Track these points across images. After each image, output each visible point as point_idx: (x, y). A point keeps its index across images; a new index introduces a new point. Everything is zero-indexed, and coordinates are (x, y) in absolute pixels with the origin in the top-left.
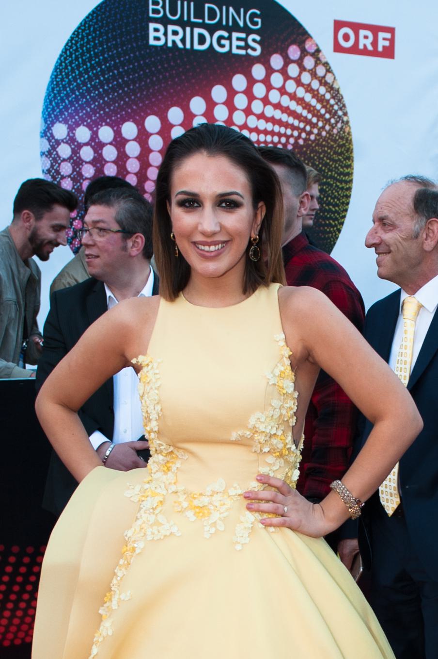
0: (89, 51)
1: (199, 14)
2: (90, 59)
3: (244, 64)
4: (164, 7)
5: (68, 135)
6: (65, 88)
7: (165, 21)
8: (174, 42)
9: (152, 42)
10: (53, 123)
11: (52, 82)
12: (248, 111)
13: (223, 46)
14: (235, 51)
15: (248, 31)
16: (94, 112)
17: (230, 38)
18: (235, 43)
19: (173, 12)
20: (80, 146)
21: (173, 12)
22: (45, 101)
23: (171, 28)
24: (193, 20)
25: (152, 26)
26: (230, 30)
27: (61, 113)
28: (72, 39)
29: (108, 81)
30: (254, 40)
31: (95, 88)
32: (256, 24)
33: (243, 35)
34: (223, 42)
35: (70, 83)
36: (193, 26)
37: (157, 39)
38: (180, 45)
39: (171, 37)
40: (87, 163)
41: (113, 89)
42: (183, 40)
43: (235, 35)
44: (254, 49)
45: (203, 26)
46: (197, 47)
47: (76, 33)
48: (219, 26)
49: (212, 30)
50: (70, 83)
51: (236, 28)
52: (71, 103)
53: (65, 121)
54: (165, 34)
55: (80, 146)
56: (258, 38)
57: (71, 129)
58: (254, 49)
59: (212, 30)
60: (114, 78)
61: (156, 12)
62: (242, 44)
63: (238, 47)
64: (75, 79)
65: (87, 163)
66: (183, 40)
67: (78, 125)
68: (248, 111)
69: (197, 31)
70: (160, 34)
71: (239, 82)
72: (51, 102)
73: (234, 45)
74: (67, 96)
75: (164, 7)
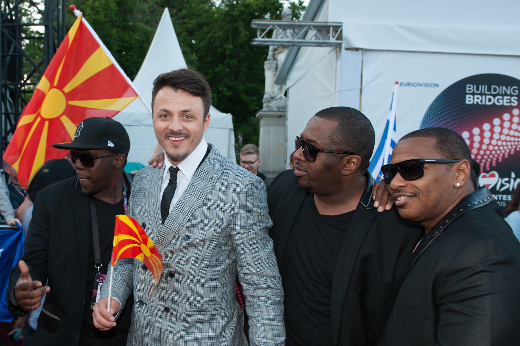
0: (439, 107)
1: (489, 90)
2: (440, 110)
3: (509, 109)
4: (473, 88)
6: (428, 122)
7: (473, 94)
8: (477, 102)
9: (467, 102)
11: (423, 120)
12: (510, 129)
13: (499, 102)
14: (505, 104)
15: (511, 95)
17: (503, 99)
18: (505, 101)
19: (477, 90)
21: (477, 90)
23: (476, 96)
24: (486, 92)
25: (467, 96)
26: (503, 95)
28: (433, 103)
29: (447, 119)
30: (514, 99)
31: (441, 121)
32: (515, 92)
33: (509, 97)
34: (500, 101)
35: (431, 120)
36: (486, 95)
37: (470, 101)
38: (480, 103)
39: (476, 100)
41: (449, 122)
42: (481, 101)
43: (505, 98)
44: (514, 103)
45: (491, 95)
46: (488, 103)
47: (435, 101)
48: (498, 94)
49: (494, 96)
50: (431, 120)
51: (506, 94)
54: (473, 99)
56: (516, 98)
58: (514, 103)
59: (494, 96)
60: (450, 117)
61: (469, 90)
62: (508, 101)
63: (507, 103)
64: (433, 118)
66: (481, 101)
68: (510, 129)
69: (488, 97)
70: (471, 99)
71: (506, 116)
73: (505, 102)
75: (473, 88)
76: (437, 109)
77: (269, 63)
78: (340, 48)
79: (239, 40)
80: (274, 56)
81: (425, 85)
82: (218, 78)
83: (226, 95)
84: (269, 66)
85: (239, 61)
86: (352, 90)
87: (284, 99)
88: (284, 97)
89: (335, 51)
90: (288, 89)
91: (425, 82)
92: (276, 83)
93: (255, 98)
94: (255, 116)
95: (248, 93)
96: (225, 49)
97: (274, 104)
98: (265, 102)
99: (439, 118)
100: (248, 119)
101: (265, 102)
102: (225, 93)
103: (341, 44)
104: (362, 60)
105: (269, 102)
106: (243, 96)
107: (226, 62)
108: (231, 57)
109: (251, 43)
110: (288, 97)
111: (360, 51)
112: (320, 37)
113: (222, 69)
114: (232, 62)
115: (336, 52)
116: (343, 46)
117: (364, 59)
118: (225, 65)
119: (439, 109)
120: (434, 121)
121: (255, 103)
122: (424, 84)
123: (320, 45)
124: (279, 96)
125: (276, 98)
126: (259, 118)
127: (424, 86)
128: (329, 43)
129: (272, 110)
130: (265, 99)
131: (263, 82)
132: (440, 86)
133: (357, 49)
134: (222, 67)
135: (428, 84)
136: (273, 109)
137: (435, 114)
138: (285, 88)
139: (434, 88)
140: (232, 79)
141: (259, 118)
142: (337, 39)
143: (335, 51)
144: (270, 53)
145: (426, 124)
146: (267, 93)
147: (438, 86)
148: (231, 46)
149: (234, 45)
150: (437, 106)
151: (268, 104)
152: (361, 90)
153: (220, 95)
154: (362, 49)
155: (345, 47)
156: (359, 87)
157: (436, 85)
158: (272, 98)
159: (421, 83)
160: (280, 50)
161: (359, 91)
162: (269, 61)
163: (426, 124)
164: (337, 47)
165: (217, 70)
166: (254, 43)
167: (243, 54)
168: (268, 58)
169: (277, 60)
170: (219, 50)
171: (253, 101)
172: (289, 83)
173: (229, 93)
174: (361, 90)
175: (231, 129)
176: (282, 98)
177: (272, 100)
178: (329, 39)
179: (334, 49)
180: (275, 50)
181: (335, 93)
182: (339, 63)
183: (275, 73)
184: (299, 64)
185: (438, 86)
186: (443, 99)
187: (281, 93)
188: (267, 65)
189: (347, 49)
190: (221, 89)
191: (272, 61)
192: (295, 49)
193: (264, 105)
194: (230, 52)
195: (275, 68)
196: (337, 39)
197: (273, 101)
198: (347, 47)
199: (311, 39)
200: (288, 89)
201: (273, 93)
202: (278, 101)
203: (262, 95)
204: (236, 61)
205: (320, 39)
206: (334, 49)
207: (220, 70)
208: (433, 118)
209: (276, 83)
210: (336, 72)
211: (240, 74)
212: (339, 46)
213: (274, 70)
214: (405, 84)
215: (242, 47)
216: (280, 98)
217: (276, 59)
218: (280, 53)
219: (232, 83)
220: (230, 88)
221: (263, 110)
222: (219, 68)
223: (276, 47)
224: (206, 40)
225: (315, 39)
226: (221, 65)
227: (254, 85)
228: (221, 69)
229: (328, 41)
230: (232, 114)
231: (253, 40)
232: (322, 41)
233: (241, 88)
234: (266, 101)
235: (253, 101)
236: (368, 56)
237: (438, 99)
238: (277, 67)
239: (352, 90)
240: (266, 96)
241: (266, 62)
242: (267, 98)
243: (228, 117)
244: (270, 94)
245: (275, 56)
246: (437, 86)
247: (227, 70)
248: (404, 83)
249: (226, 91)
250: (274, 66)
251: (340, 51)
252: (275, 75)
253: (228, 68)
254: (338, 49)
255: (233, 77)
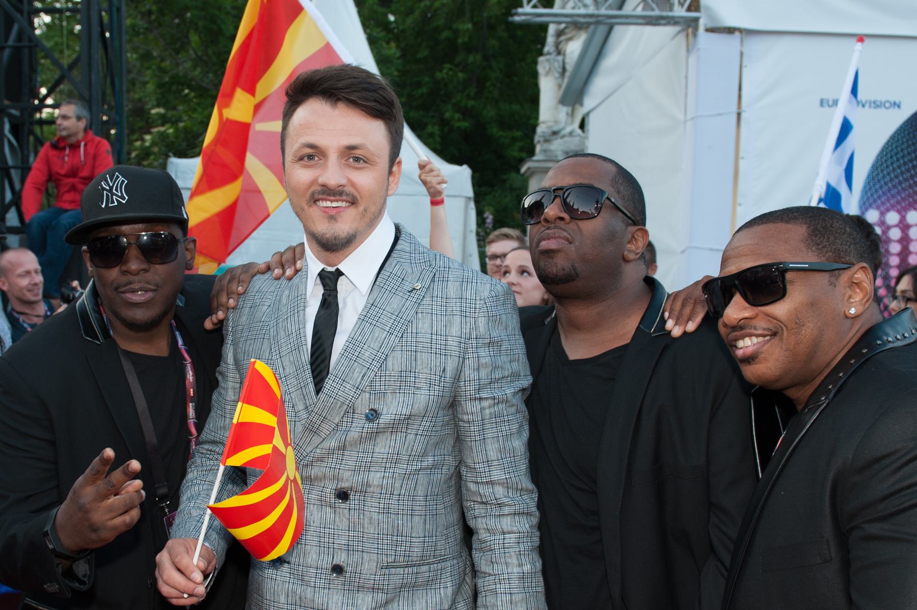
0: (902, 150)
2: (903, 157)
5: (880, 219)
6: (879, 181)
10: (867, 210)
11: (868, 177)
16: (904, 199)
20: (889, 228)
22: (862, 191)
27: (875, 201)
28: (888, 141)
35: (884, 177)
40: (894, 241)
47: (893, 137)
50: (884, 177)
52: (884, 193)
53: (878, 208)
55: (889, 228)
57: (883, 214)
64: (889, 174)
65: (894, 241)
67: (888, 210)
72: (866, 193)
74: (881, 187)
76: (896, 154)
77: (548, 60)
78: (696, 29)
79: (485, 14)
80: (557, 45)
81: (872, 105)
82: (442, 92)
83: (458, 128)
84: (547, 67)
85: (485, 58)
86: (720, 115)
87: (579, 135)
88: (579, 131)
89: (684, 33)
90: (588, 114)
91: (872, 99)
92: (563, 101)
93: (518, 134)
94: (518, 170)
95: (503, 124)
96: (456, 32)
97: (557, 146)
98: (539, 142)
99: (902, 173)
100: (504, 177)
101: (539, 142)
102: (457, 124)
103: (696, 20)
104: (742, 54)
105: (547, 141)
106: (494, 130)
107: (458, 59)
108: (469, 49)
109: (510, 19)
110: (588, 130)
111: (737, 34)
112: (654, 6)
113: (451, 73)
114: (471, 59)
115: (687, 35)
116: (702, 23)
117: (744, 51)
118: (457, 65)
119: (901, 154)
120: (891, 180)
121: (519, 144)
122: (870, 103)
123: (654, 22)
124: (568, 129)
125: (563, 133)
126: (527, 175)
127: (870, 106)
128: (673, 18)
129: (554, 159)
130: (540, 136)
131: (534, 100)
132: (902, 106)
133: (730, 31)
134: (450, 69)
135: (878, 103)
136: (556, 157)
137: (892, 164)
138: (580, 112)
139: (891, 110)
140: (472, 94)
141: (527, 175)
142: (689, 9)
143: (684, 33)
144: (550, 39)
145: (874, 185)
146: (544, 122)
147: (899, 107)
148: (470, 26)
149: (474, 24)
150: (896, 147)
151: (546, 146)
152: (739, 115)
153: (446, 129)
154: (740, 30)
155: (706, 25)
156: (734, 109)
157: (895, 103)
158: (555, 133)
159: (864, 102)
160: (570, 33)
161: (734, 117)
162: (548, 57)
163: (874, 185)
164: (689, 26)
165: (439, 75)
166: (517, 19)
167: (493, 42)
168: (546, 49)
169: (564, 55)
170: (446, 34)
171: (514, 139)
172: (589, 102)
173: (464, 124)
174: (739, 115)
175: (469, 198)
176: (575, 134)
177: (553, 138)
178: (671, 9)
179: (683, 30)
180: (560, 34)
181: (685, 122)
182: (692, 59)
183: (560, 80)
184: (610, 61)
185: (899, 107)
186: (909, 134)
187: (572, 122)
188: (543, 65)
189: (711, 30)
190: (447, 115)
191: (553, 56)
192: (602, 29)
193: (538, 148)
194: (466, 39)
195: (560, 70)
196: (689, 9)
197: (556, 139)
198: (709, 26)
199: (634, 9)
200: (588, 114)
201: (556, 122)
202: (566, 139)
203: (532, 129)
204: (479, 57)
205: (653, 10)
206: (683, 30)
207: (445, 76)
208: (889, 174)
209: (563, 101)
210: (686, 77)
211: (488, 84)
212: (693, 24)
213: (557, 75)
214: (831, 103)
215: (492, 28)
216: (571, 134)
217: (562, 52)
218: (570, 39)
219: (471, 103)
220: (466, 113)
221: (535, 158)
222: (445, 71)
223: (563, 26)
224: (417, 14)
225: (644, 9)
226: (448, 66)
227: (516, 107)
228: (447, 73)
229: (670, 14)
230: (471, 166)
231: (514, 11)
232: (657, 13)
233: (490, 112)
234: (542, 139)
235: (514, 139)
236: (755, 45)
237: (898, 135)
238: (564, 69)
239: (720, 115)
240: (541, 129)
241: (541, 59)
242: (543, 132)
243: (464, 172)
244: (550, 124)
245: (561, 46)
246: (896, 107)
247: (460, 75)
248: (828, 101)
249: (459, 120)
250: (557, 66)
251: (695, 34)
252: (560, 86)
253: (461, 71)
254: (690, 30)
255: (472, 90)
